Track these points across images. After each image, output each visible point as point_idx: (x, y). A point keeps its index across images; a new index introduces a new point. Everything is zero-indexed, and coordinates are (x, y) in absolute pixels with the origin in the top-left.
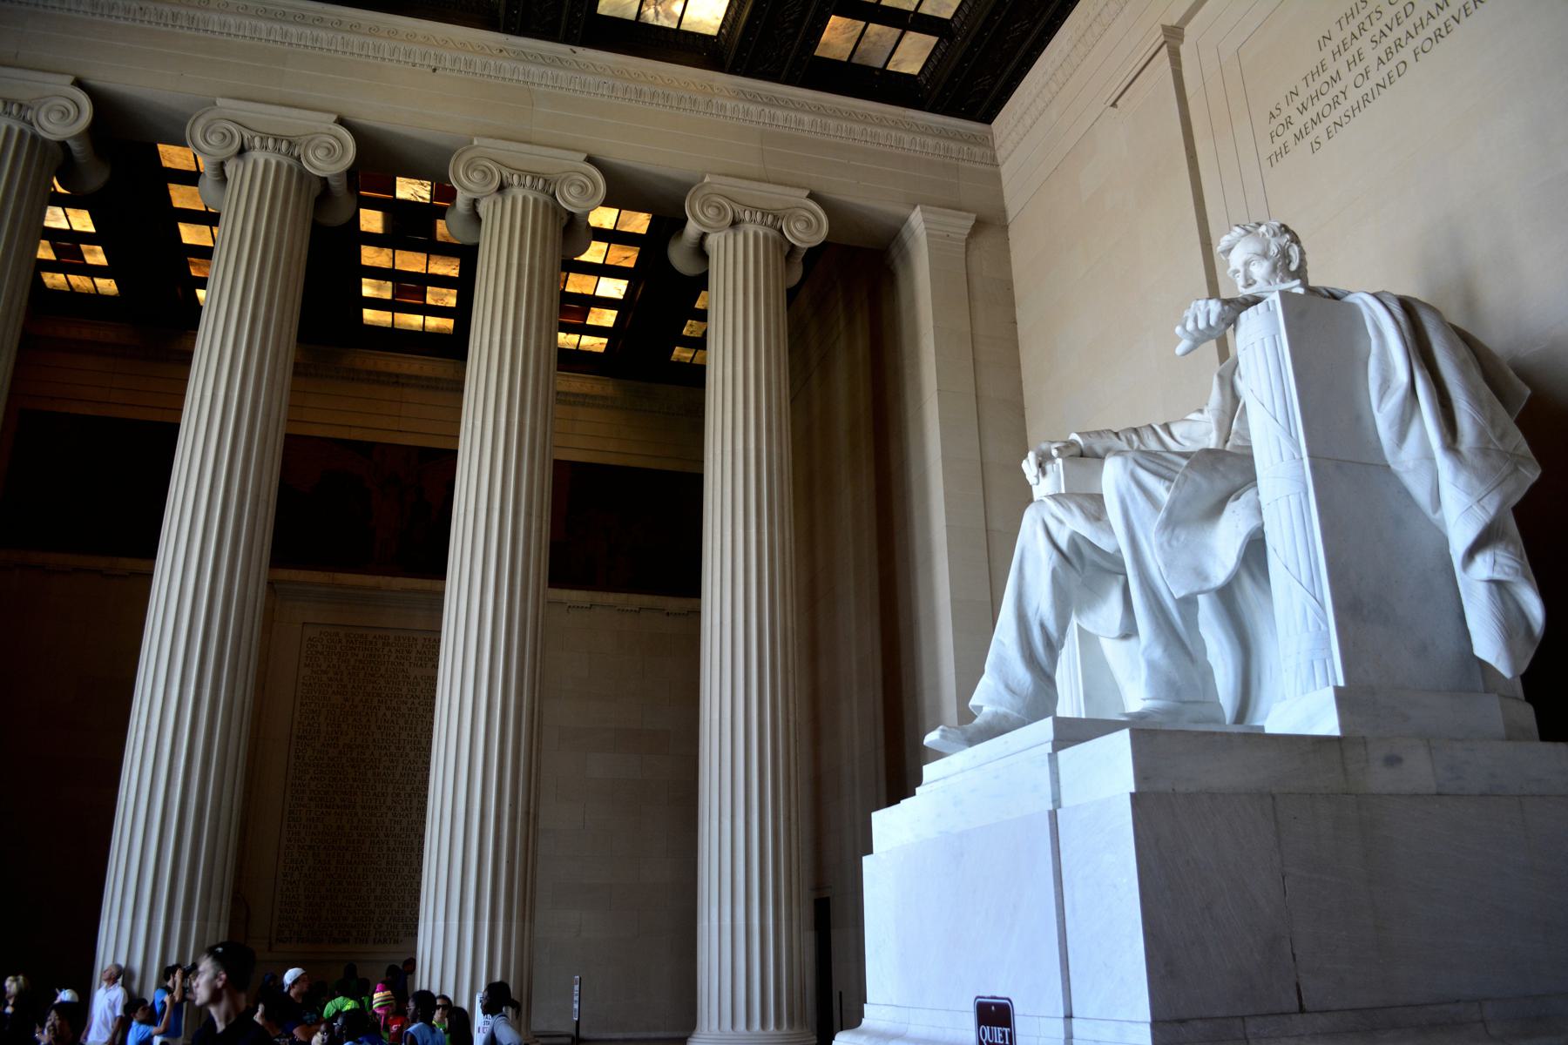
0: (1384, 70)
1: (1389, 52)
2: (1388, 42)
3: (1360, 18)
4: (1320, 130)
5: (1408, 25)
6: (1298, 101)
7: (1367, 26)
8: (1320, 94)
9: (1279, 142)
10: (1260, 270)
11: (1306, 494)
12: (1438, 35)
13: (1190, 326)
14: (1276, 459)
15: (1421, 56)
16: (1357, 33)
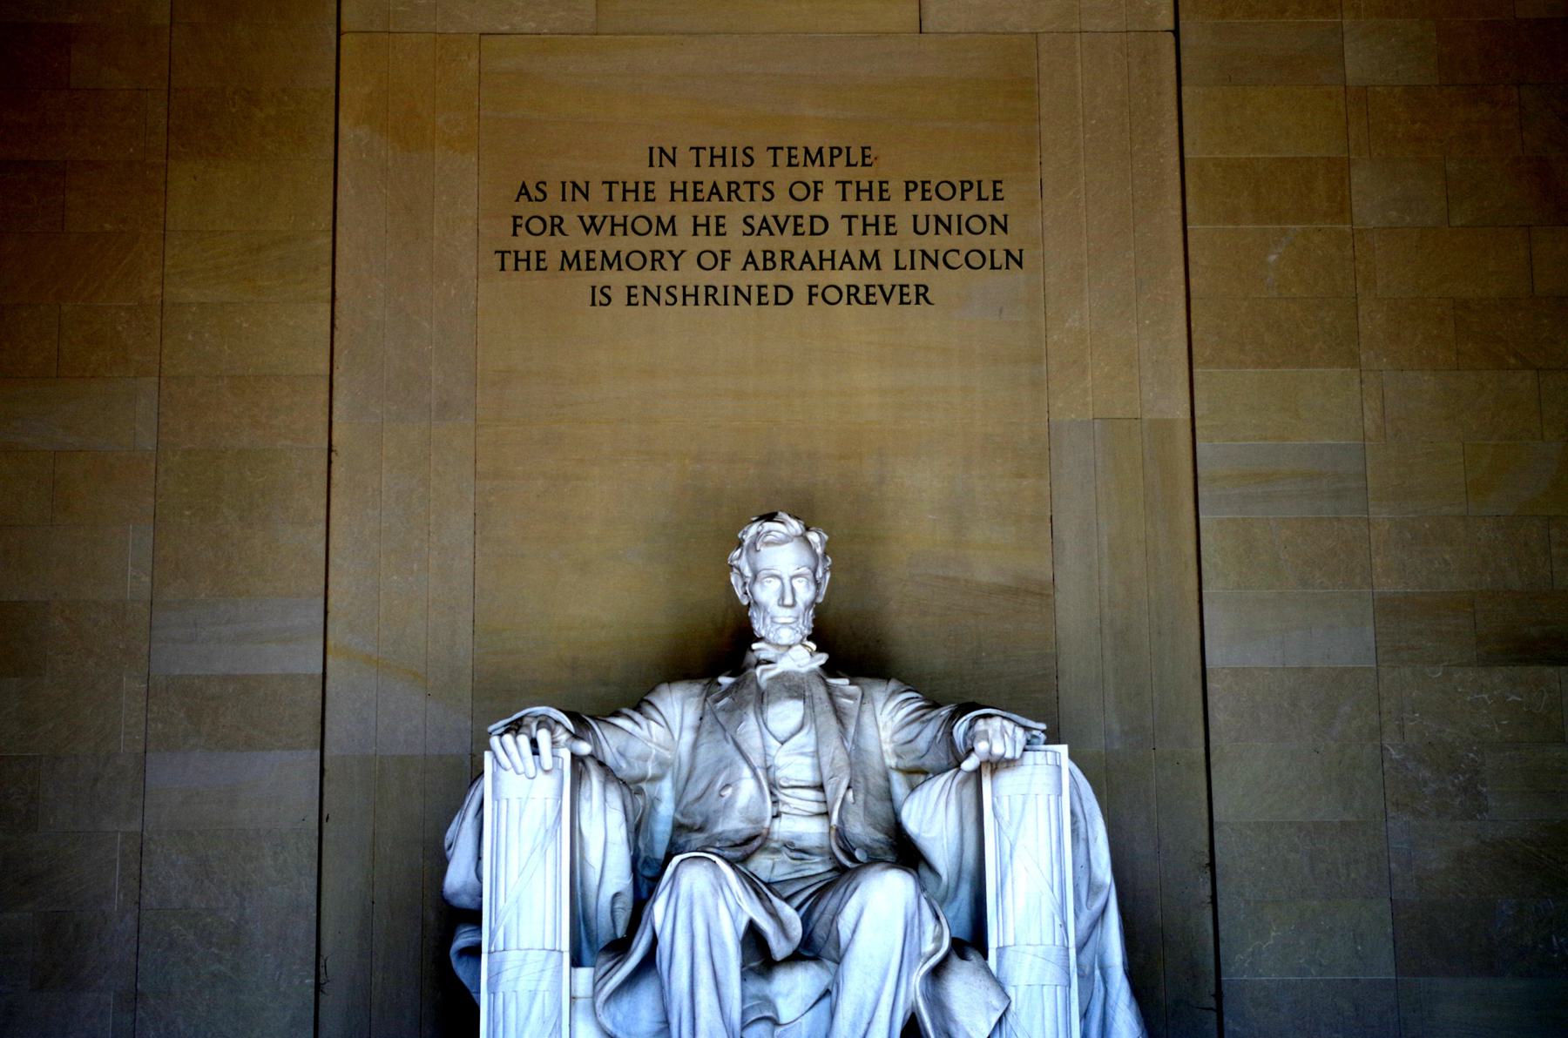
0: (753, 278)
1: (768, 256)
2: (779, 243)
3: (740, 174)
4: (617, 280)
5: (814, 245)
6: (583, 207)
7: (744, 192)
8: (626, 226)
9: (525, 243)
10: (805, 593)
11: (1070, 986)
12: (852, 293)
13: (998, 750)
14: (1048, 940)
15: (817, 300)
16: (725, 196)
